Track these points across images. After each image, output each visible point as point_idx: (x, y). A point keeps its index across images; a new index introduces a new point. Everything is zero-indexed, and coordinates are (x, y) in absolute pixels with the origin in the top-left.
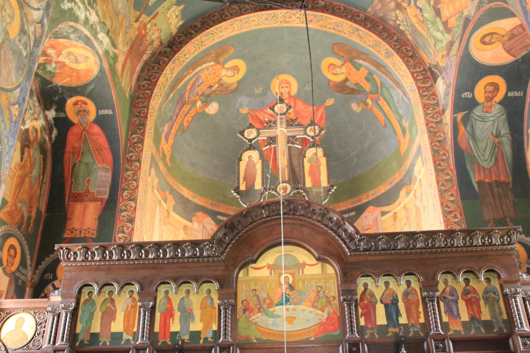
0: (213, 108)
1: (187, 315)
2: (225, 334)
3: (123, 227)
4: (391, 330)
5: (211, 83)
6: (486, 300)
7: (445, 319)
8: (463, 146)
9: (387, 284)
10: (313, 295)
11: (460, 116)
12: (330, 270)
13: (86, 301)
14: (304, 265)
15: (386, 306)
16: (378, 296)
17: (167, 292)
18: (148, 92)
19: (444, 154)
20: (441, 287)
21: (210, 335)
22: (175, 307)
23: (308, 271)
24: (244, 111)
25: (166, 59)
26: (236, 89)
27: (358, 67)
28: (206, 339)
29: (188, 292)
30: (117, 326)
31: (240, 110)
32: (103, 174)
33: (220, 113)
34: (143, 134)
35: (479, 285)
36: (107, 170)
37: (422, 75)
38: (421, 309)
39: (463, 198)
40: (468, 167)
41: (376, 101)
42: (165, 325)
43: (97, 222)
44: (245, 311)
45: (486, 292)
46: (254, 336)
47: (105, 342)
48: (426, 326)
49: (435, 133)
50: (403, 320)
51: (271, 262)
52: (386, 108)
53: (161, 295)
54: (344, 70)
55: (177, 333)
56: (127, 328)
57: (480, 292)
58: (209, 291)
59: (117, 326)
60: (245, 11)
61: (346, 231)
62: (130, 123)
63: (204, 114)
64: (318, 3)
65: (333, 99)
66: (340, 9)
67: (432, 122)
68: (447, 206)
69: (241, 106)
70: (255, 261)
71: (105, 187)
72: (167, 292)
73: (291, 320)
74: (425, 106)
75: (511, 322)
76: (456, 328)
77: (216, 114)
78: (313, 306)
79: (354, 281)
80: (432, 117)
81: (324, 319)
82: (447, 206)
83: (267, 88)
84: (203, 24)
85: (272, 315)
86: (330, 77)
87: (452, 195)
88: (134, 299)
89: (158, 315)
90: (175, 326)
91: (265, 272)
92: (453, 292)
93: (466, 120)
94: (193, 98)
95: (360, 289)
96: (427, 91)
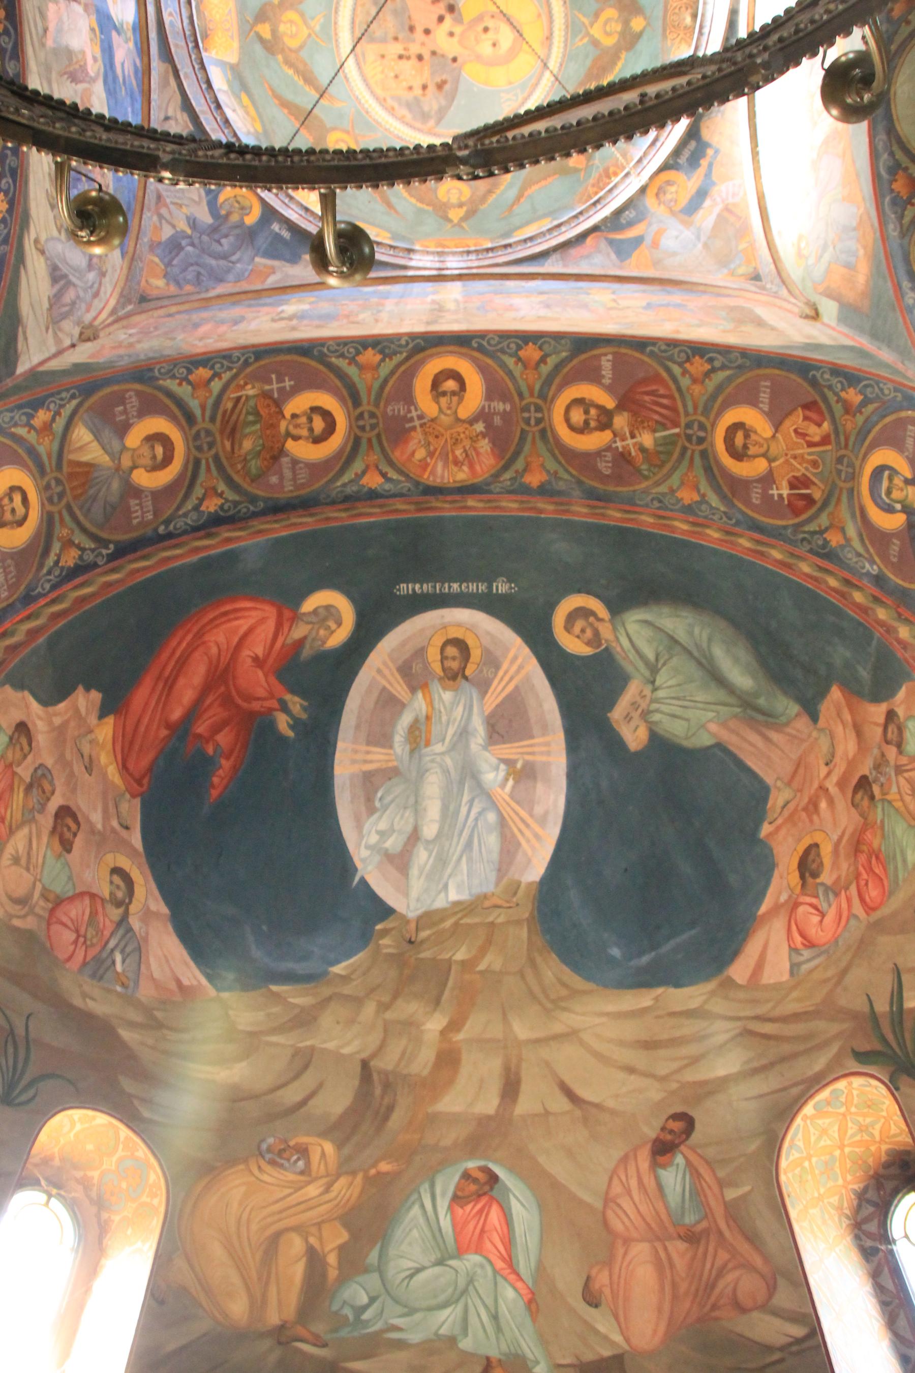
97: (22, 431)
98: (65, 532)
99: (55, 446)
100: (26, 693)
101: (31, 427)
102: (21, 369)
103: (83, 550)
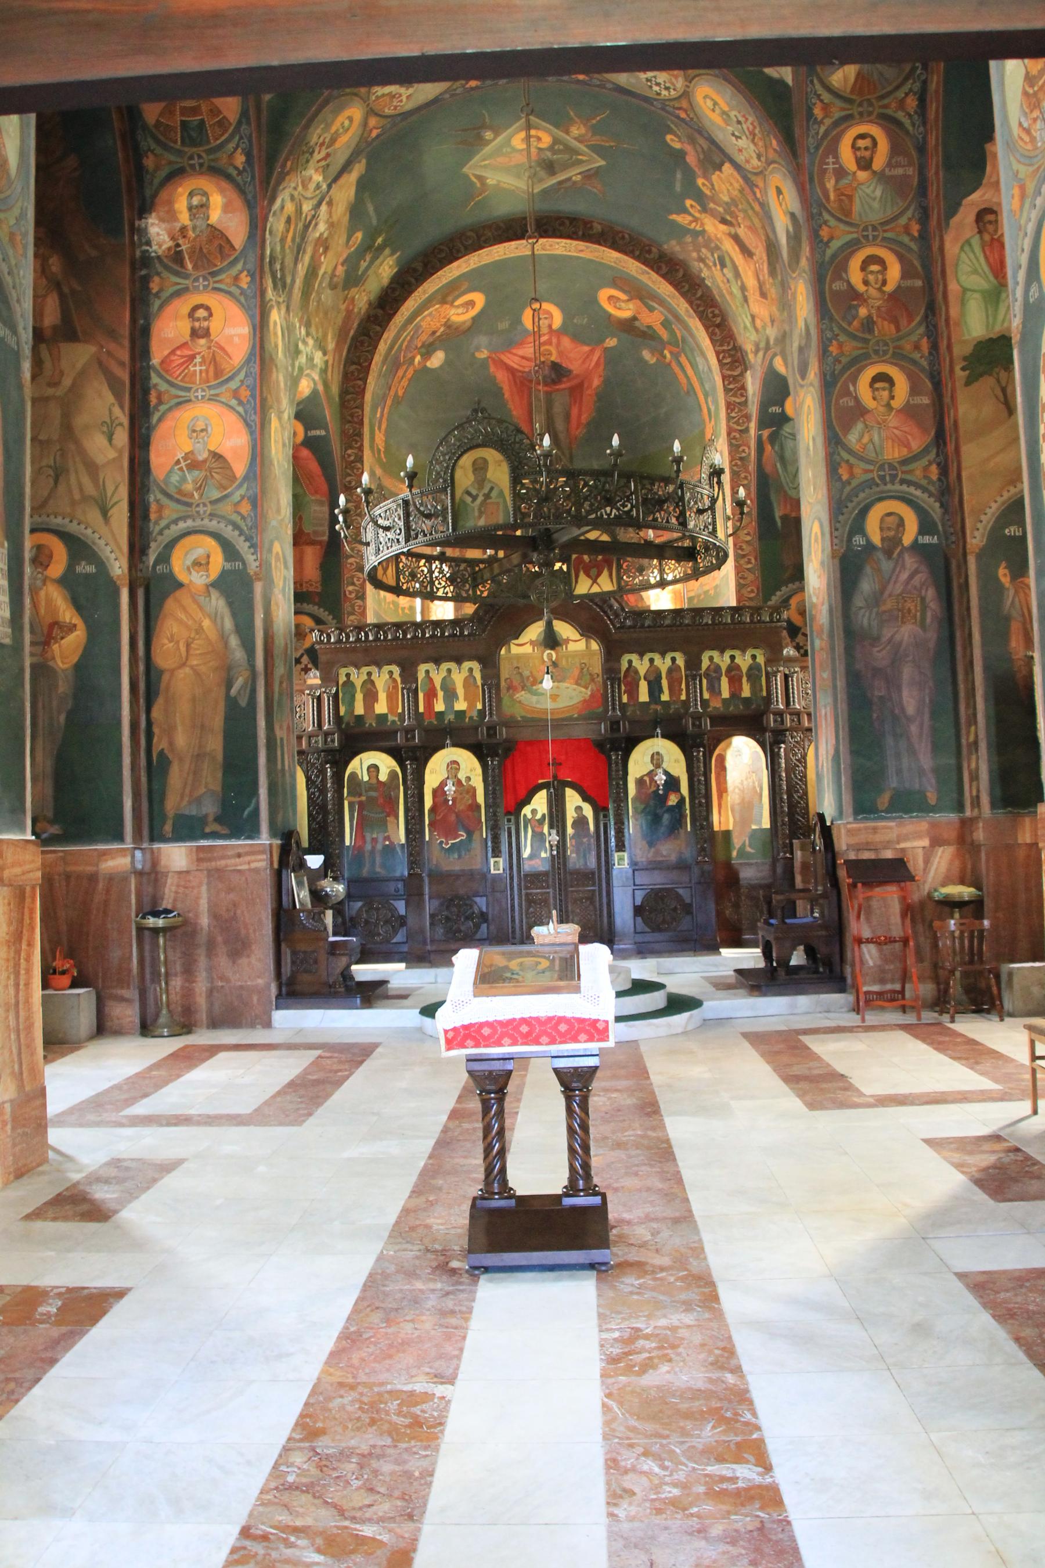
0: (437, 359)
1: (451, 695)
2: (491, 714)
3: (353, 577)
4: (653, 707)
5: (434, 328)
6: (749, 677)
7: (706, 696)
8: (768, 469)
9: (652, 661)
10: (576, 672)
11: (766, 433)
12: (595, 646)
13: (345, 683)
14: (567, 641)
15: (649, 683)
16: (642, 672)
17: (427, 672)
18: (360, 383)
19: (746, 478)
20: (705, 663)
21: (475, 714)
22: (438, 686)
23: (572, 647)
24: (483, 354)
25: (378, 328)
26: (469, 328)
27: (651, 309)
28: (471, 718)
29: (449, 671)
30: (381, 707)
31: (477, 355)
32: (317, 508)
33: (448, 362)
34: (361, 449)
35: (744, 661)
36: (321, 503)
37: (730, 356)
38: (683, 686)
39: (760, 538)
40: (773, 497)
41: (676, 356)
42: (429, 705)
43: (318, 573)
44: (508, 689)
45: (750, 668)
46: (518, 713)
47: (371, 723)
48: (686, 704)
49: (739, 446)
50: (665, 697)
51: (534, 638)
52: (690, 372)
53: (421, 675)
54: (631, 305)
55: (441, 713)
56: (392, 707)
57: (744, 670)
58: (471, 670)
59: (381, 707)
60: (485, 242)
61: (611, 607)
62: (343, 433)
63: (425, 370)
64: (591, 228)
65: (615, 340)
66: (623, 238)
67: (736, 430)
68: (741, 548)
69: (478, 349)
70: (517, 638)
71: (322, 525)
72: (427, 672)
73: (554, 697)
74: (730, 406)
75: (768, 700)
76: (716, 704)
77: (441, 367)
78: (577, 684)
79: (618, 660)
80: (737, 423)
81: (587, 697)
82: (741, 548)
83: (517, 321)
84: (425, 265)
85: (536, 693)
86: (611, 310)
87: (748, 534)
88: (395, 681)
89: (421, 696)
90: (440, 706)
91: (528, 649)
92: (718, 668)
93: (773, 438)
94: (410, 355)
95: (625, 665)
96: (734, 384)
97: (822, 129)
98: (893, 105)
99: (839, 103)
100: (964, 202)
101: (822, 122)
102: (790, 83)
103: (911, 90)
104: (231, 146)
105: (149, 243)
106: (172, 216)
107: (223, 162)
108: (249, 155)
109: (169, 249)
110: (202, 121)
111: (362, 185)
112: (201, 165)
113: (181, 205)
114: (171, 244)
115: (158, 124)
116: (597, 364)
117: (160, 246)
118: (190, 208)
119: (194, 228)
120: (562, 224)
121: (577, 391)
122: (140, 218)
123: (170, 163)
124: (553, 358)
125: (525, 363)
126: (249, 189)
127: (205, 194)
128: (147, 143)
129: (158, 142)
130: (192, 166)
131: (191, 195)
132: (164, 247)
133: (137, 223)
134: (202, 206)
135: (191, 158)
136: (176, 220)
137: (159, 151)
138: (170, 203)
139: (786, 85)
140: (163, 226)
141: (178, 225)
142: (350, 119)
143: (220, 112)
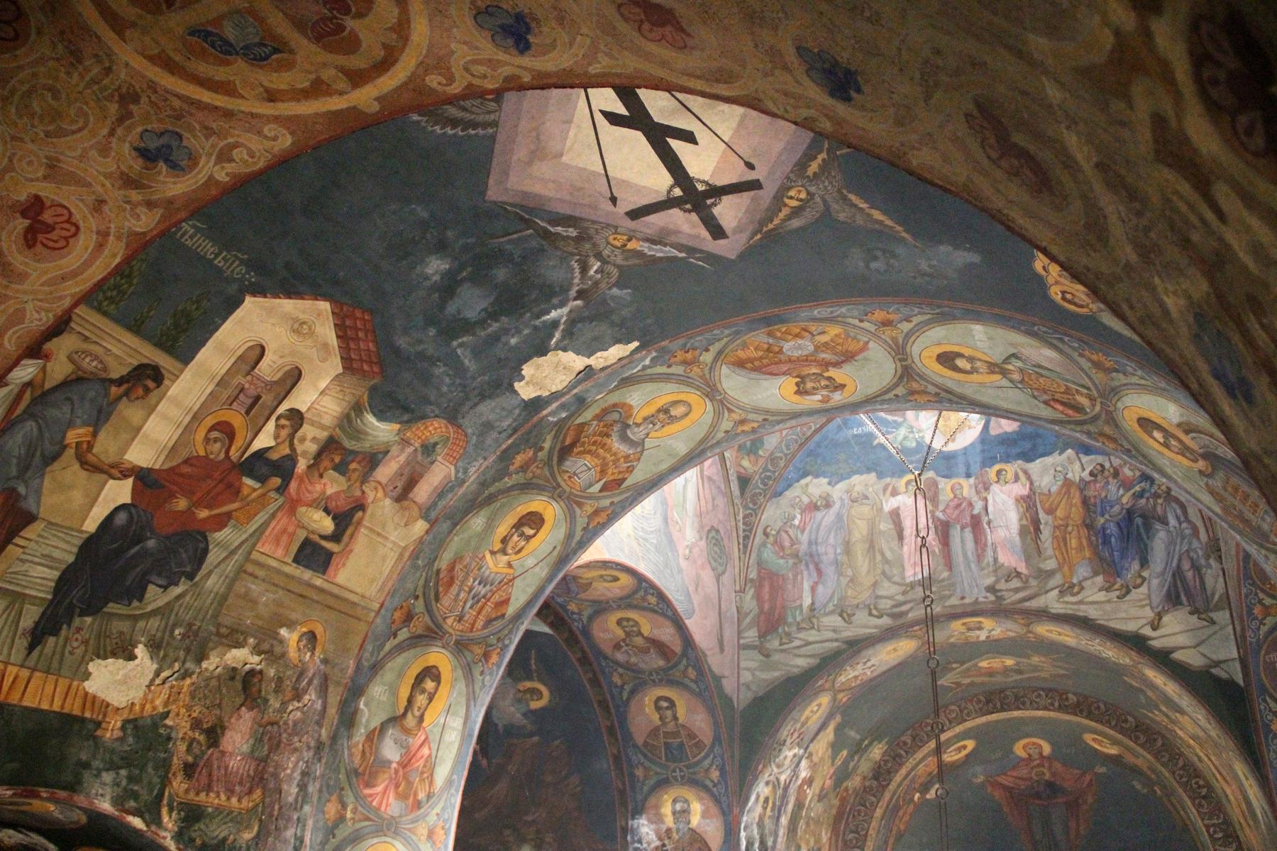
24: (981, 779)
31: (974, 780)
63: (924, 802)
64: (1067, 699)
69: (975, 776)
104: (707, 762)
105: (640, 841)
106: (659, 819)
107: (700, 777)
108: (722, 770)
109: (657, 848)
110: (682, 744)
111: (838, 730)
112: (682, 777)
113: (667, 810)
114: (658, 843)
115: (646, 744)
116: (1090, 784)
117: (649, 844)
118: (674, 813)
119: (678, 830)
120: (1039, 695)
121: (1073, 806)
122: (633, 819)
123: (657, 773)
124: (1047, 776)
125: (1020, 782)
126: (723, 799)
127: (686, 801)
128: (637, 758)
129: (645, 756)
130: (675, 778)
131: (675, 801)
132: (653, 846)
133: (630, 822)
134: (684, 811)
135: (674, 771)
136: (663, 822)
137: (647, 764)
138: (657, 807)
139: (1237, 685)
140: (652, 827)
141: (664, 828)
142: (819, 705)
143: (695, 736)
